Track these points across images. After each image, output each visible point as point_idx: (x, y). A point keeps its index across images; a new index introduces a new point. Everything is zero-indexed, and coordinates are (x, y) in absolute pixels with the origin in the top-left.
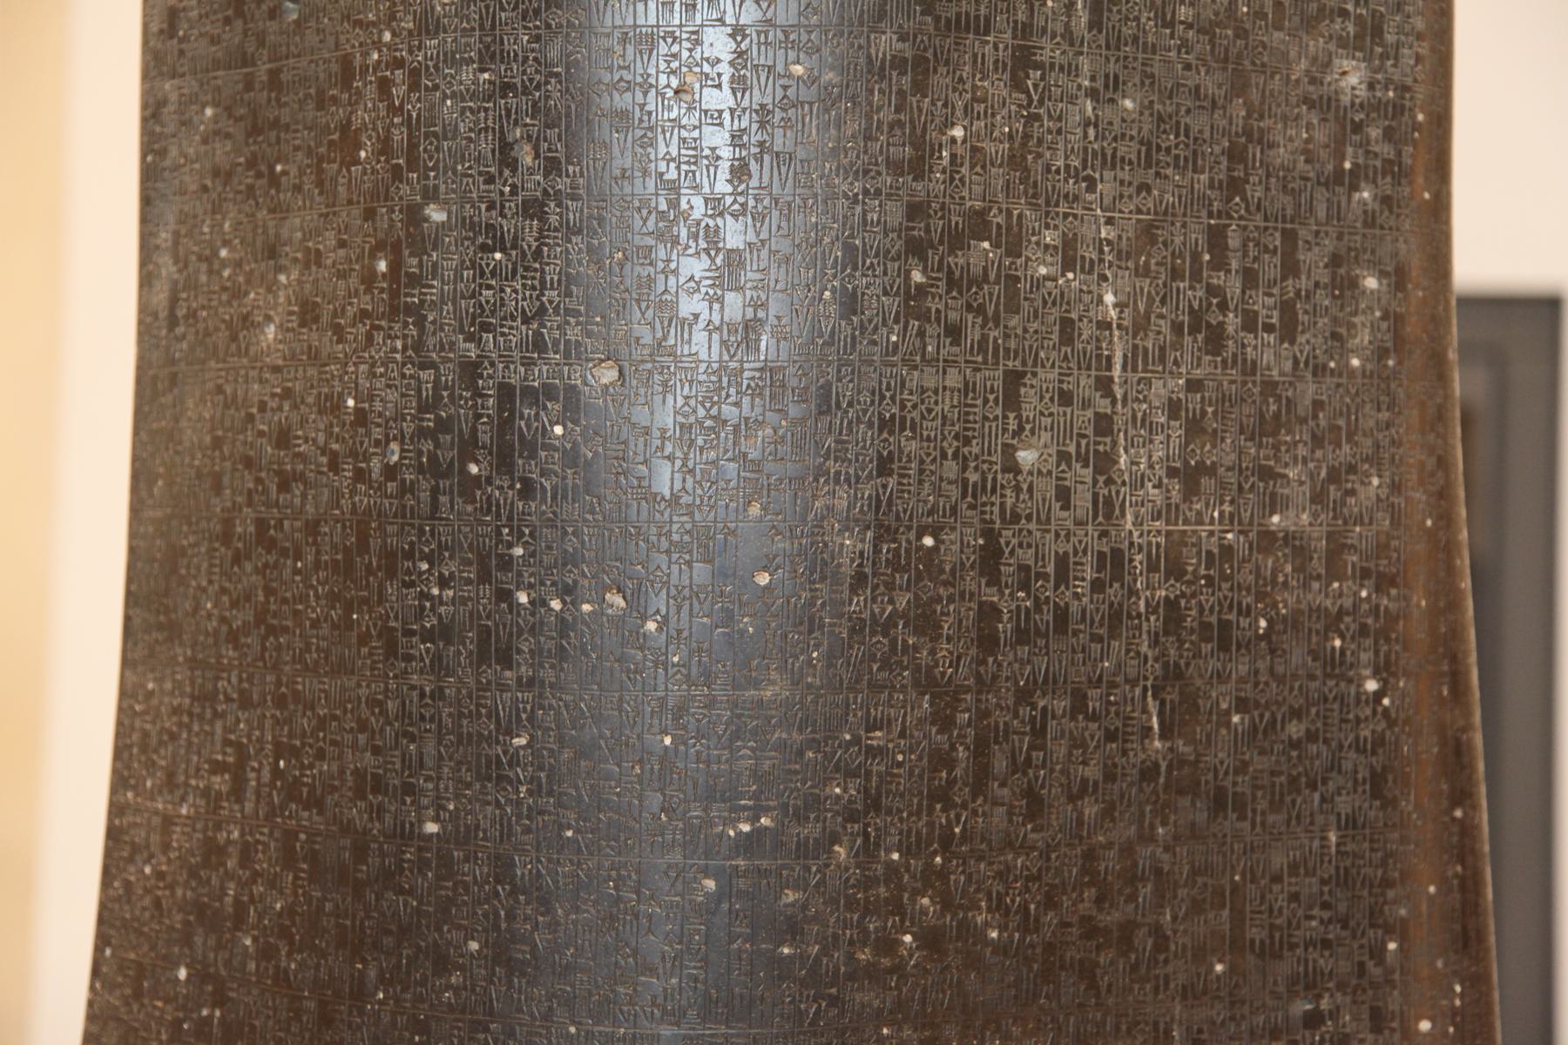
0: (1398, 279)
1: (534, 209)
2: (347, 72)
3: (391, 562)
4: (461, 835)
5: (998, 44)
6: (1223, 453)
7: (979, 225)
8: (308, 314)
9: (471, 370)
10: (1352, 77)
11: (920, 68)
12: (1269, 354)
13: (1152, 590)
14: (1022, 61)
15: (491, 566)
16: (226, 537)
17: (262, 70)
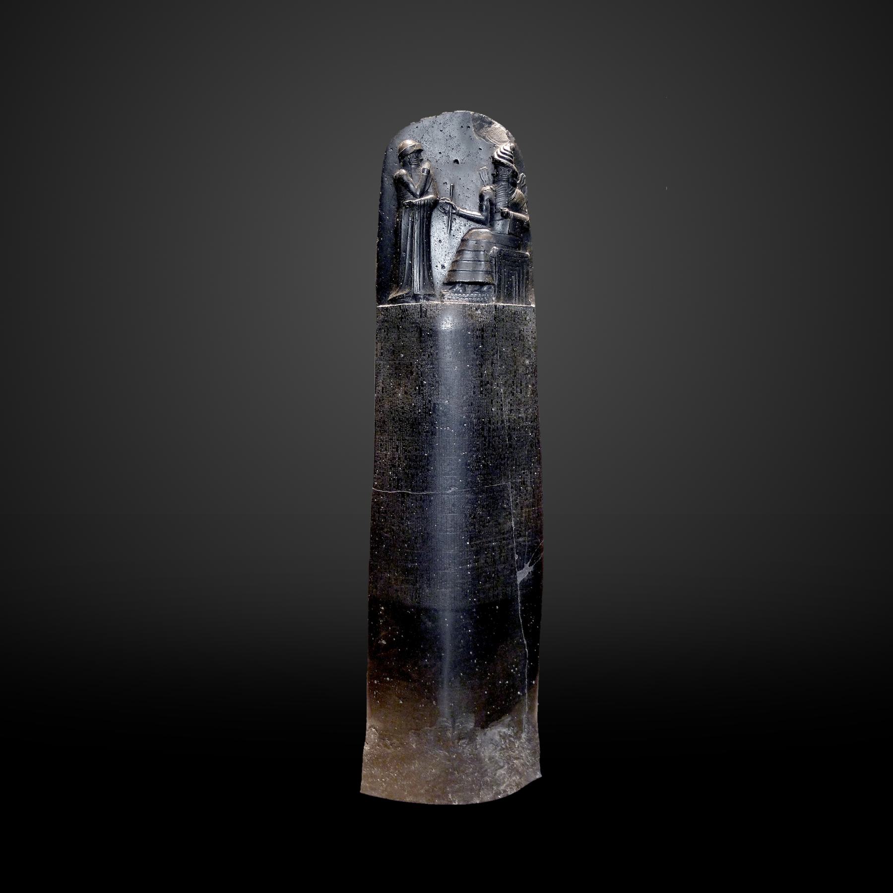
0: (533, 385)
1: (437, 382)
2: (411, 364)
3: (419, 424)
4: (430, 455)
5: (489, 362)
6: (514, 408)
7: (488, 383)
8: (406, 393)
9: (430, 401)
10: (527, 362)
11: (481, 365)
12: (519, 396)
13: (507, 424)
14: (492, 363)
15: (433, 424)
16: (394, 419)
17: (397, 362)
